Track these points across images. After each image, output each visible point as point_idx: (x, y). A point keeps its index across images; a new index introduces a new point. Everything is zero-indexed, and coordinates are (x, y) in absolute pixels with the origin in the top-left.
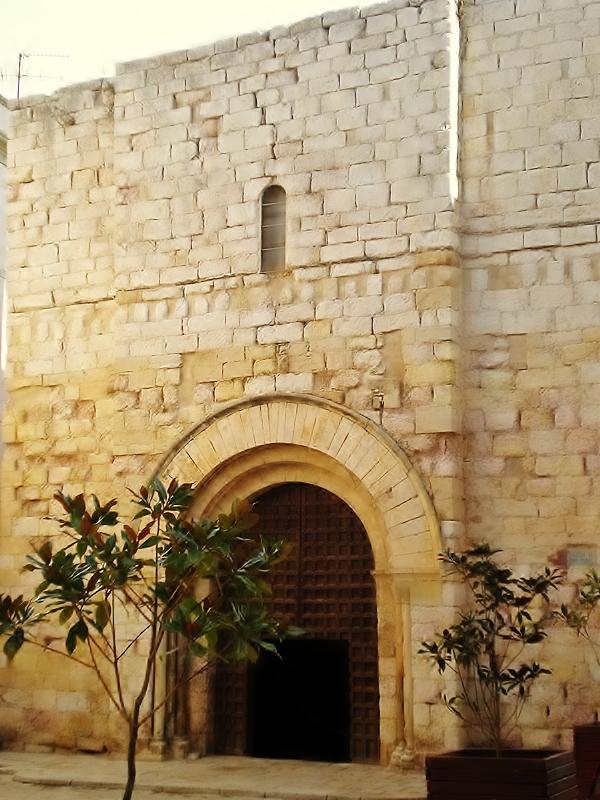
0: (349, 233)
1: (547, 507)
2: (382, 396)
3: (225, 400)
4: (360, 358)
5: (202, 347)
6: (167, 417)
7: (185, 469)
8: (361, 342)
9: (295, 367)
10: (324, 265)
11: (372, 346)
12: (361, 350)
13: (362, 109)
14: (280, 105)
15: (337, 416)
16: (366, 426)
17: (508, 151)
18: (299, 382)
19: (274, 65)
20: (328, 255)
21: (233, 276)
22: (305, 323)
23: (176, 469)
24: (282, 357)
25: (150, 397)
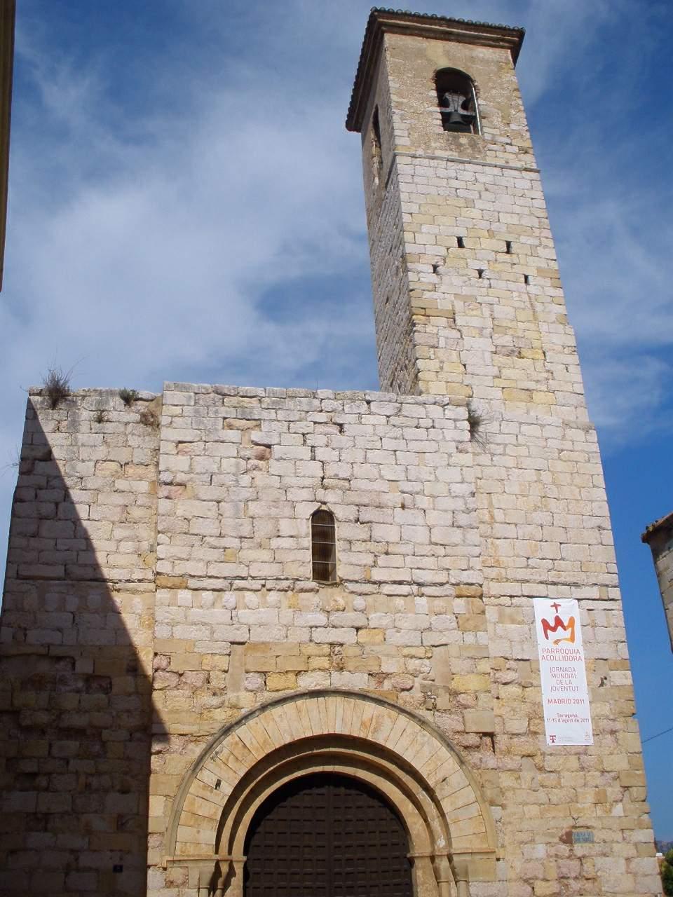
0: (398, 561)
1: (556, 795)
2: (435, 699)
3: (277, 691)
4: (413, 664)
5: (254, 638)
6: (215, 701)
7: (236, 753)
8: (413, 651)
9: (350, 665)
10: (374, 583)
11: (422, 656)
12: (411, 658)
13: (403, 468)
14: (329, 449)
15: (394, 713)
16: (422, 723)
17: (505, 523)
18: (359, 681)
19: (322, 417)
20: (377, 575)
21: (287, 579)
22: (358, 629)
23: (226, 751)
24: (336, 657)
25: (194, 678)
